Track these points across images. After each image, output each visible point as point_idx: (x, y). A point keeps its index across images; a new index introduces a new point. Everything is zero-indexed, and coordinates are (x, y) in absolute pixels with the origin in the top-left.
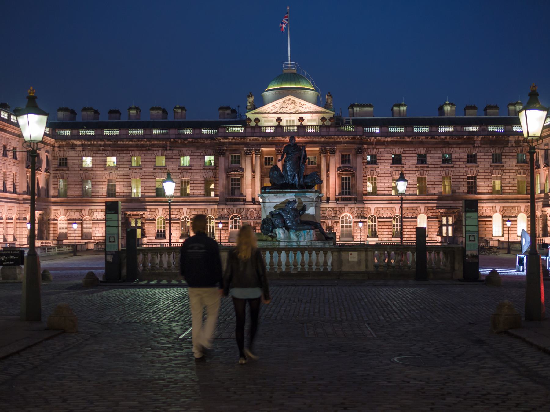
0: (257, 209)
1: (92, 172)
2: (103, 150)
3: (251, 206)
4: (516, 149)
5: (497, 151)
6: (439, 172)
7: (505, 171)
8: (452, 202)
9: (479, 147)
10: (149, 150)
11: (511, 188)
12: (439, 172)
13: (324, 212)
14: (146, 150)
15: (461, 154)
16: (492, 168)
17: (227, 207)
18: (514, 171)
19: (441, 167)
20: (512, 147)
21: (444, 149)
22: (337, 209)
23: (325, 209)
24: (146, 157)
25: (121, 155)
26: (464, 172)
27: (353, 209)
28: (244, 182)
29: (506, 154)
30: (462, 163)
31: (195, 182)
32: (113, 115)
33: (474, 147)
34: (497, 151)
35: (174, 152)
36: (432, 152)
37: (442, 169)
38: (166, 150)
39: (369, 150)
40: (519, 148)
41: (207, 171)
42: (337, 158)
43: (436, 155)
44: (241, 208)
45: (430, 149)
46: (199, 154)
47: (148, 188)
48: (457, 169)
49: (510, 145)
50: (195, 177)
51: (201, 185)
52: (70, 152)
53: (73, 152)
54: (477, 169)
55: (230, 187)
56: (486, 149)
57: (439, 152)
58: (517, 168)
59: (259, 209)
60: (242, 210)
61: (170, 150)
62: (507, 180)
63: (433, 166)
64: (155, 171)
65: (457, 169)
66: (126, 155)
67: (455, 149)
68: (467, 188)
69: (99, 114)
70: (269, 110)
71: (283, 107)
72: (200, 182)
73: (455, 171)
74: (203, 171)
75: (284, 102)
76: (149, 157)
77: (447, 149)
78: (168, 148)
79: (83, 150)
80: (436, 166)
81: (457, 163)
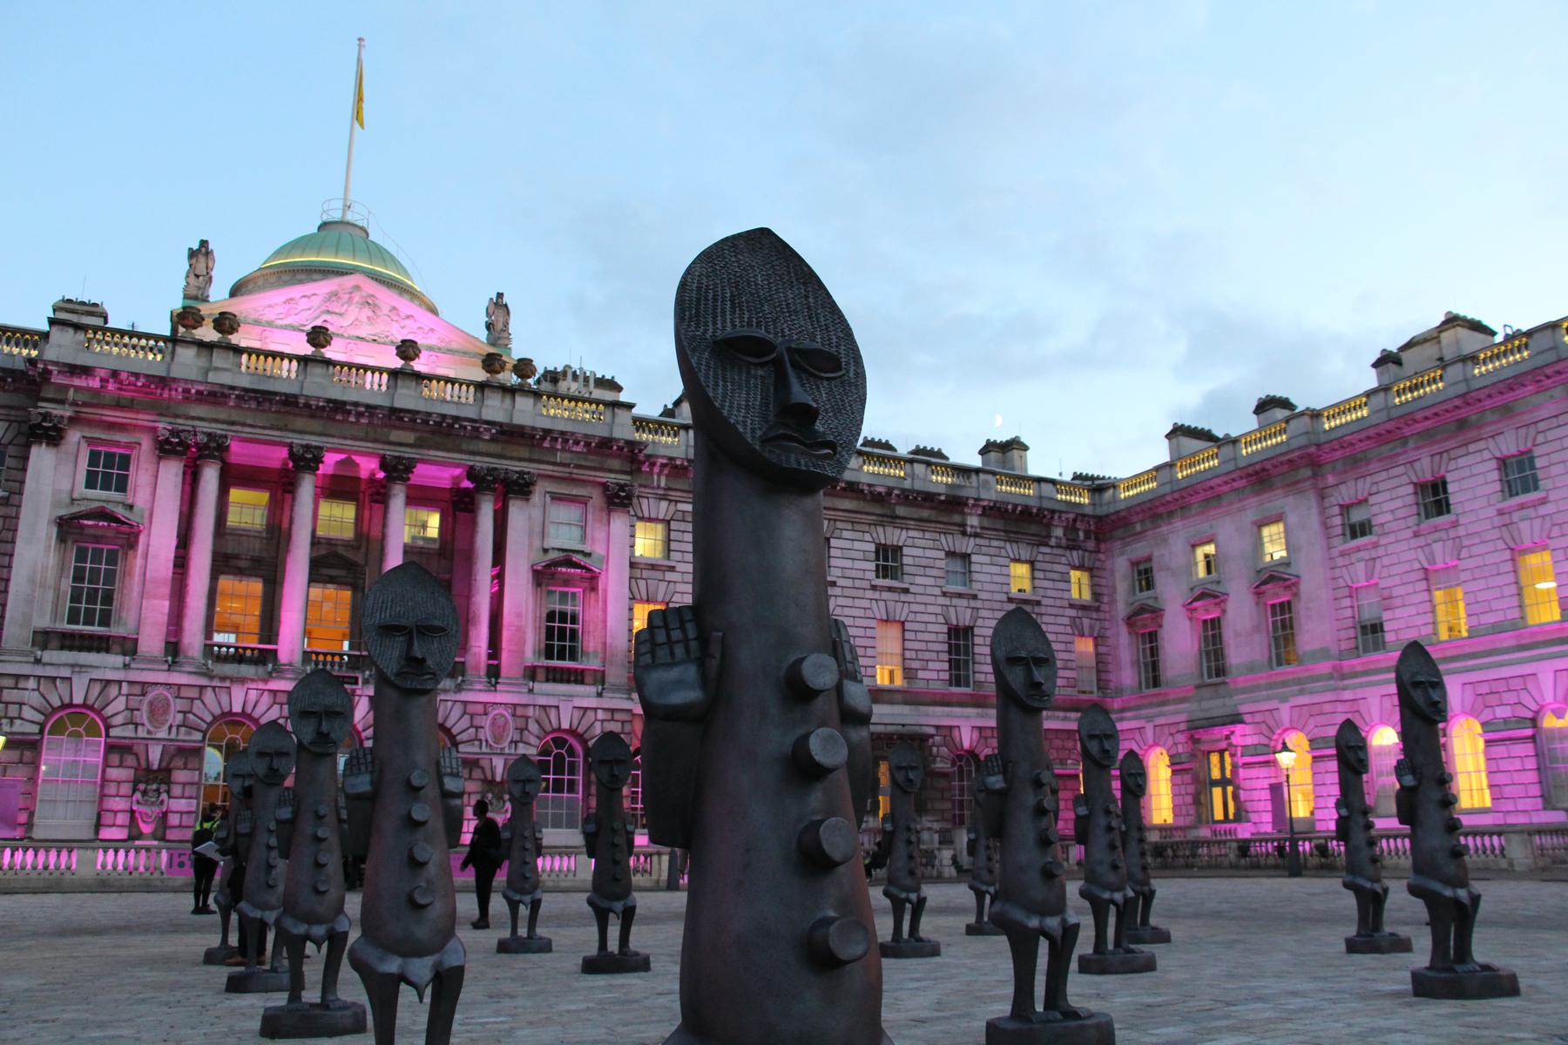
0: (184, 692)
3: (161, 677)
4: (1068, 553)
6: (866, 603)
8: (906, 709)
9: (976, 535)
12: (866, 603)
13: (477, 721)
15: (929, 553)
17: (39, 671)
18: (1066, 621)
19: (874, 588)
20: (1059, 546)
21: (880, 529)
22: (530, 711)
23: (480, 709)
26: (938, 610)
27: (590, 714)
28: (137, 571)
29: (1048, 566)
30: (930, 581)
33: (964, 533)
36: (846, 534)
37: (876, 595)
39: (644, 502)
42: (537, 513)
43: (857, 545)
44: (107, 683)
45: (839, 525)
48: (919, 599)
49: (1053, 542)
54: (973, 603)
55: (67, 584)
56: (994, 543)
57: (867, 537)
58: (1073, 613)
59: (194, 693)
60: (113, 691)
63: (849, 583)
65: (919, 599)
67: (912, 533)
68: (946, 666)
70: (269, 316)
71: (328, 312)
73: (914, 607)
75: (334, 295)
77: (889, 529)
80: (858, 583)
81: (919, 580)
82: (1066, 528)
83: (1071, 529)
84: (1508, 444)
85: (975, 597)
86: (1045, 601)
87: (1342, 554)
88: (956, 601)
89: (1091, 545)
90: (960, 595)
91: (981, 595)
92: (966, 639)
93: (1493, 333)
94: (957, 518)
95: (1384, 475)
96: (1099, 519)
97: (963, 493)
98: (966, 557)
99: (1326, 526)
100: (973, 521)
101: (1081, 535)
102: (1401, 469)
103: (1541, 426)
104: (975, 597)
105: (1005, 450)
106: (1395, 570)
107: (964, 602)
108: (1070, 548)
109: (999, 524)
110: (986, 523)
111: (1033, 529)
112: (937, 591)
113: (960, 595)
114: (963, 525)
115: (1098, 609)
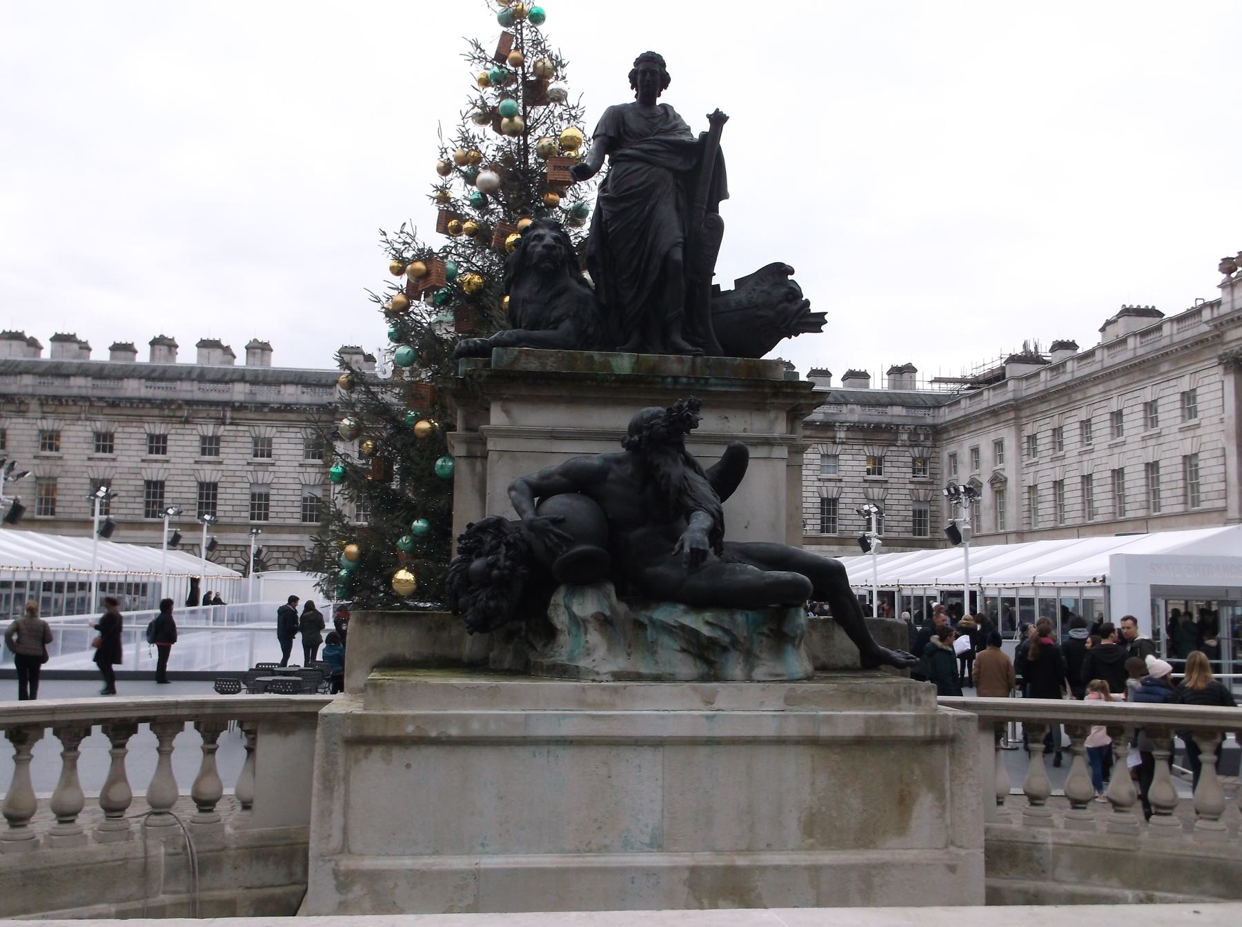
1: (59, 462)
2: (87, 419)
5: (877, 451)
7: (891, 491)
9: (843, 443)
10: (187, 421)
11: (901, 524)
14: (180, 423)
16: (867, 485)
18: (907, 492)
24: (180, 437)
25: (126, 430)
26: (815, 489)
31: (281, 492)
32: (118, 354)
33: (834, 443)
34: (877, 451)
35: (240, 428)
38: (224, 424)
40: (916, 449)
41: (309, 470)
46: (293, 435)
47: (180, 501)
49: (899, 443)
50: (282, 481)
51: (293, 498)
52: (14, 420)
53: (21, 420)
54: (838, 484)
58: (912, 486)
61: (231, 424)
62: (894, 507)
64: (197, 466)
66: (135, 430)
69: (89, 349)
72: (291, 492)
74: (299, 469)
76: (186, 438)
78: (228, 421)
79: (43, 418)
82: (910, 434)
83: (914, 433)
84: (1082, 415)
85: (840, 480)
86: (891, 480)
87: (1028, 466)
88: (826, 484)
89: (929, 443)
90: (830, 480)
91: (845, 479)
92: (834, 505)
93: (1161, 315)
94: (830, 434)
95: (1042, 422)
96: (934, 427)
97: (836, 418)
98: (836, 456)
99: (1020, 448)
100: (841, 435)
101: (922, 438)
102: (1047, 420)
103: (1096, 406)
104: (840, 480)
105: (902, 372)
106: (1045, 479)
107: (833, 484)
108: (910, 446)
109: (860, 435)
110: (850, 435)
111: (886, 436)
112: (814, 478)
113: (830, 480)
114: (834, 438)
115: (932, 483)
